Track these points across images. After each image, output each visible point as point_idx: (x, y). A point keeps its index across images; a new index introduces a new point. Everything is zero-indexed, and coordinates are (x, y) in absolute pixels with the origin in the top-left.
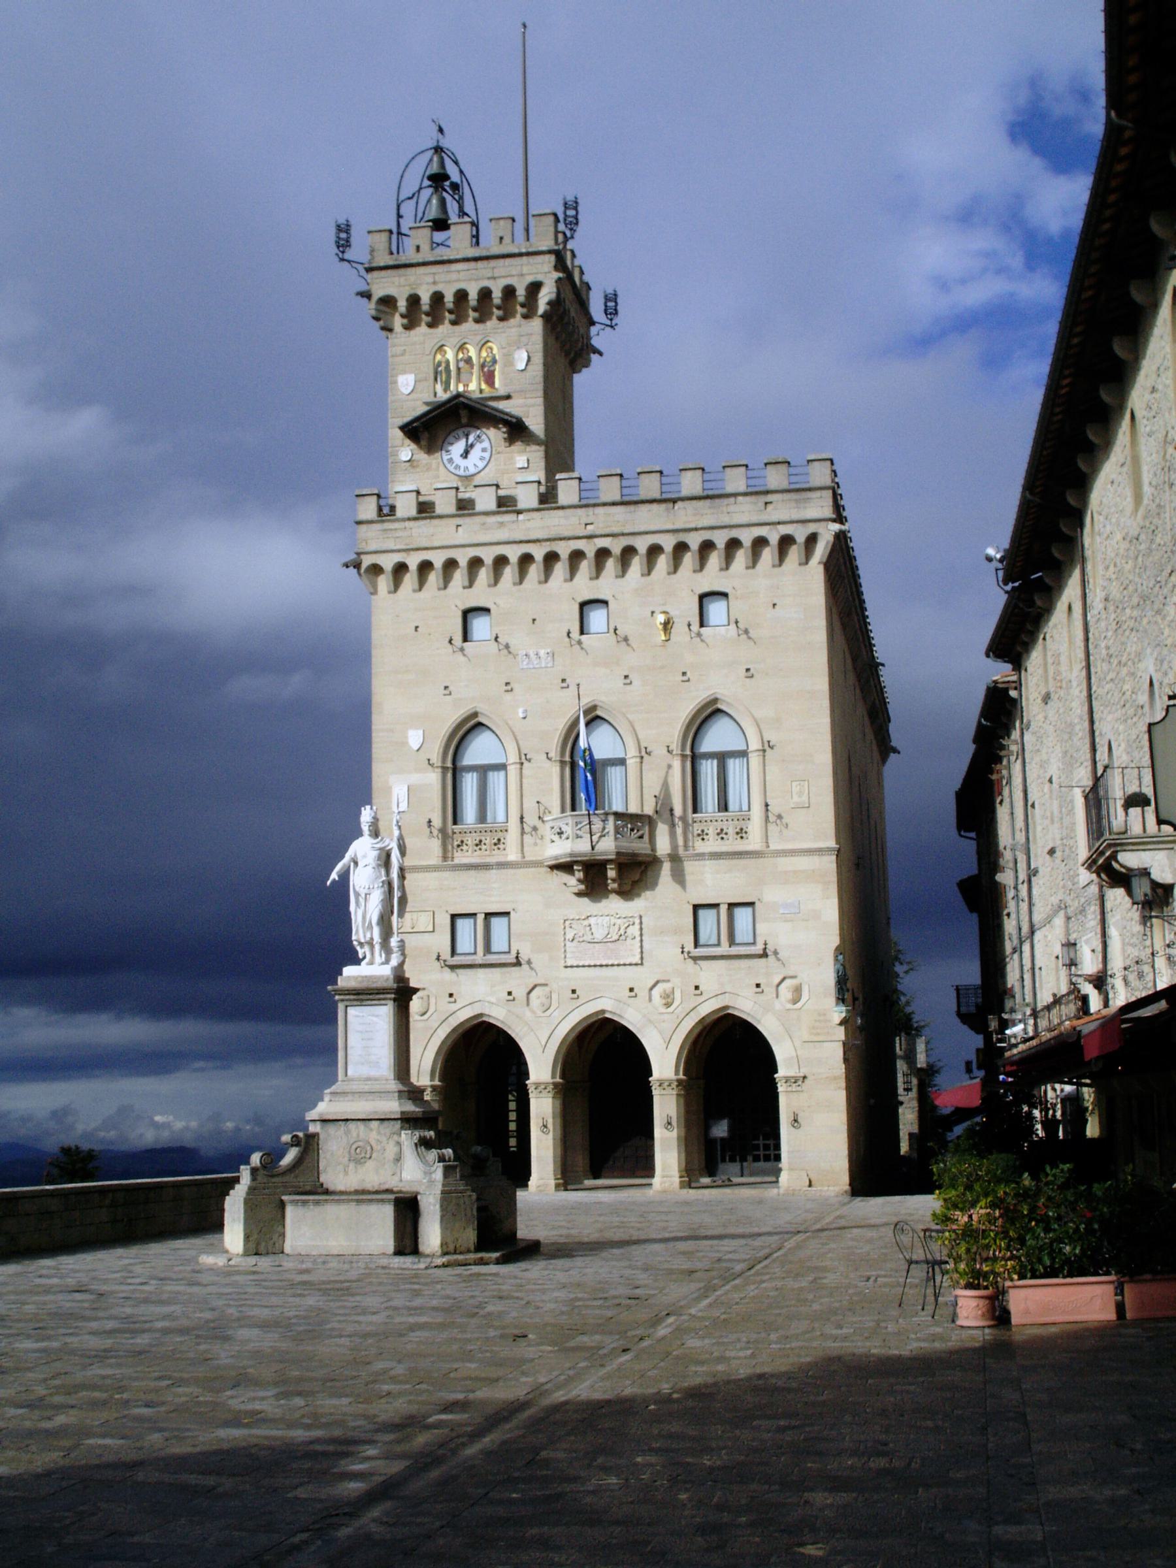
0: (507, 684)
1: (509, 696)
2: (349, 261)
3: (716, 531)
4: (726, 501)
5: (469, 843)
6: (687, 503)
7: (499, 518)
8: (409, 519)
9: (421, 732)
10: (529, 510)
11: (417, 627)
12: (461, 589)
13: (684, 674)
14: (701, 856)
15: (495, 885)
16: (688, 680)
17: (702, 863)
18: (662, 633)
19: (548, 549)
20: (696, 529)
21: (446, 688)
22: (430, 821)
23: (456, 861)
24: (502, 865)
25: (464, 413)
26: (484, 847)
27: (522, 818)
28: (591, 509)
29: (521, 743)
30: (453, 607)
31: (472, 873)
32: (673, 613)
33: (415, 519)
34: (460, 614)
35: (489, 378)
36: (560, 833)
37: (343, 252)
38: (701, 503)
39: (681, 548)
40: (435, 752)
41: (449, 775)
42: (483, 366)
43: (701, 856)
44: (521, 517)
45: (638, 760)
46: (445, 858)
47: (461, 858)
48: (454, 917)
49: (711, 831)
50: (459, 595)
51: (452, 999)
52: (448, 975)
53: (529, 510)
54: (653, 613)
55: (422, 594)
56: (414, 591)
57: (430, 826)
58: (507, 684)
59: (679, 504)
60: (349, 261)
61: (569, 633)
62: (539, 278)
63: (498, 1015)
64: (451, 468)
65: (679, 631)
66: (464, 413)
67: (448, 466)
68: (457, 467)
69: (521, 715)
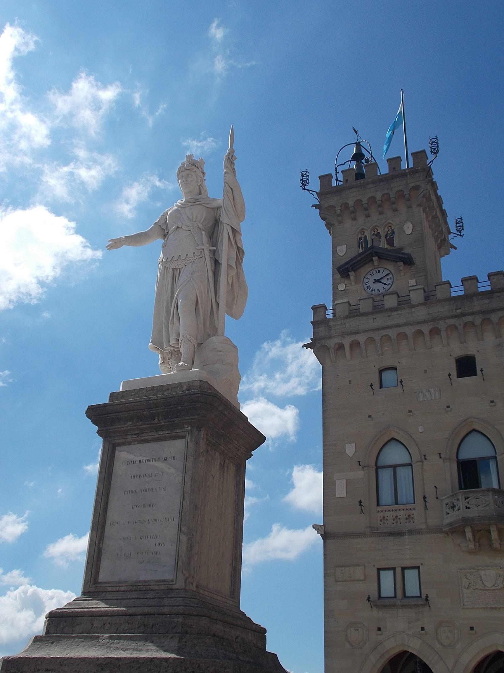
2: (308, 190)
10: (418, 305)
11: (350, 381)
15: (408, 547)
19: (432, 326)
22: (360, 502)
24: (411, 532)
25: (375, 259)
27: (424, 498)
35: (390, 242)
36: (453, 507)
37: (305, 186)
42: (386, 236)
48: (379, 570)
51: (379, 632)
52: (376, 613)
58: (410, 411)
60: (308, 190)
61: (449, 375)
62: (418, 183)
63: (414, 646)
66: (375, 259)
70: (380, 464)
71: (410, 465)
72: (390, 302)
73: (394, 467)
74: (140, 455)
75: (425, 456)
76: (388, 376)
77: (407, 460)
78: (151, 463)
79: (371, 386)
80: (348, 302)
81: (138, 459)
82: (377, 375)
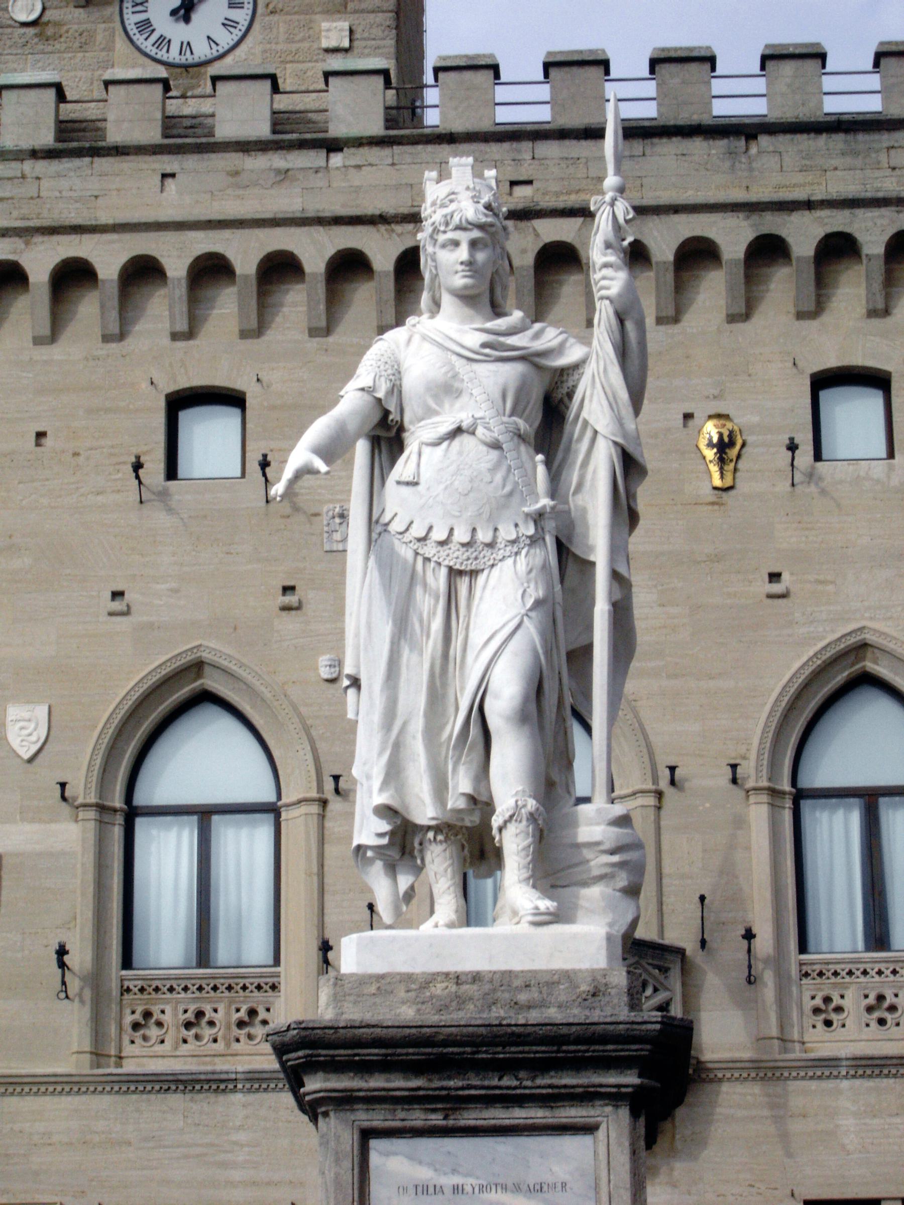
0: (288, 589)
1: (289, 624)
3: (860, 212)
4: (886, 139)
5: (167, 1018)
6: (782, 141)
7: (279, 160)
8: (34, 154)
9: (42, 712)
12: (166, 341)
13: (775, 577)
14: (826, 1067)
15: (242, 1137)
16: (783, 596)
17: (830, 1084)
18: (714, 469)
20: (809, 205)
21: (117, 595)
22: (62, 952)
23: (129, 1067)
26: (207, 1033)
28: (526, 145)
29: (322, 746)
30: (145, 385)
31: (176, 1100)
32: (744, 418)
33: (50, 154)
34: (162, 403)
38: (822, 141)
39: (768, 251)
40: (80, 768)
41: (117, 832)
43: (826, 1067)
44: (337, 160)
45: (651, 801)
46: (98, 1055)
47: (144, 1057)
49: (852, 1001)
50: (158, 353)
53: (359, 142)
54: (688, 417)
55: (56, 352)
56: (38, 341)
57: (62, 965)
59: (764, 140)
64: (147, 45)
65: (763, 459)
67: (139, 39)
68: (163, 42)
69: (325, 673)
70: (141, 798)
71: (273, 810)
72: (241, 114)
73: (205, 815)
74: (454, 1171)
75: (336, 778)
76: (212, 441)
77: (260, 790)
78: (486, 1196)
79: (137, 466)
80: (59, 89)
81: (449, 1181)
82: (159, 420)
